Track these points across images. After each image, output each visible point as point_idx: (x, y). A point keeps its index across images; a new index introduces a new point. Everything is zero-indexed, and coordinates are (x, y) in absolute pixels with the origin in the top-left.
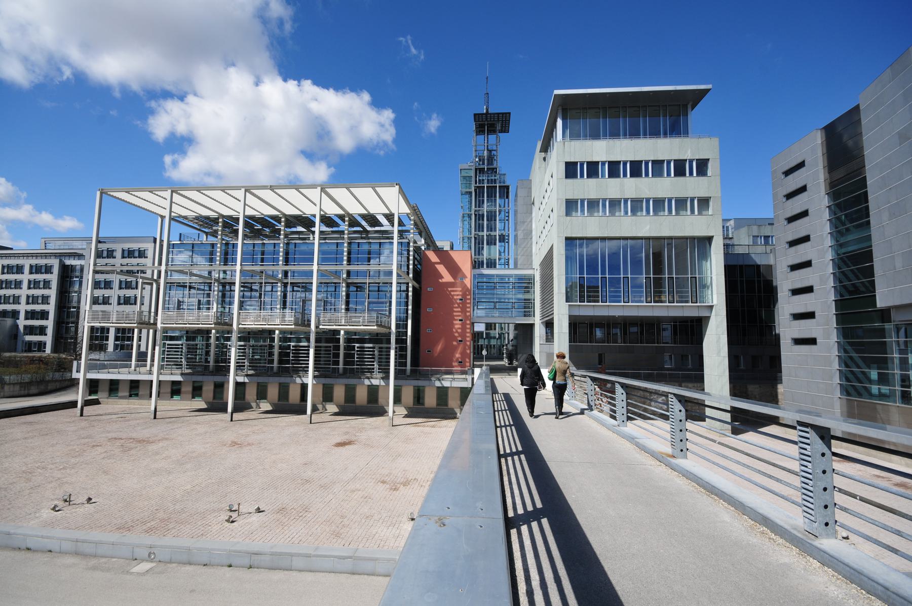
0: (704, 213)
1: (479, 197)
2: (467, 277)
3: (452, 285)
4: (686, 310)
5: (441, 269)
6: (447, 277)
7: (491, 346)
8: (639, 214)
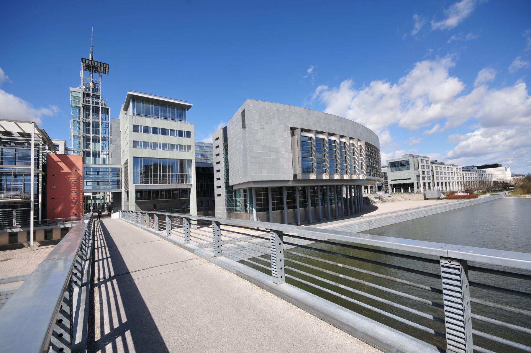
0: (189, 151)
1: (86, 111)
2: (79, 170)
3: (68, 174)
4: (184, 186)
5: (62, 165)
6: (66, 169)
7: (96, 204)
8: (165, 149)
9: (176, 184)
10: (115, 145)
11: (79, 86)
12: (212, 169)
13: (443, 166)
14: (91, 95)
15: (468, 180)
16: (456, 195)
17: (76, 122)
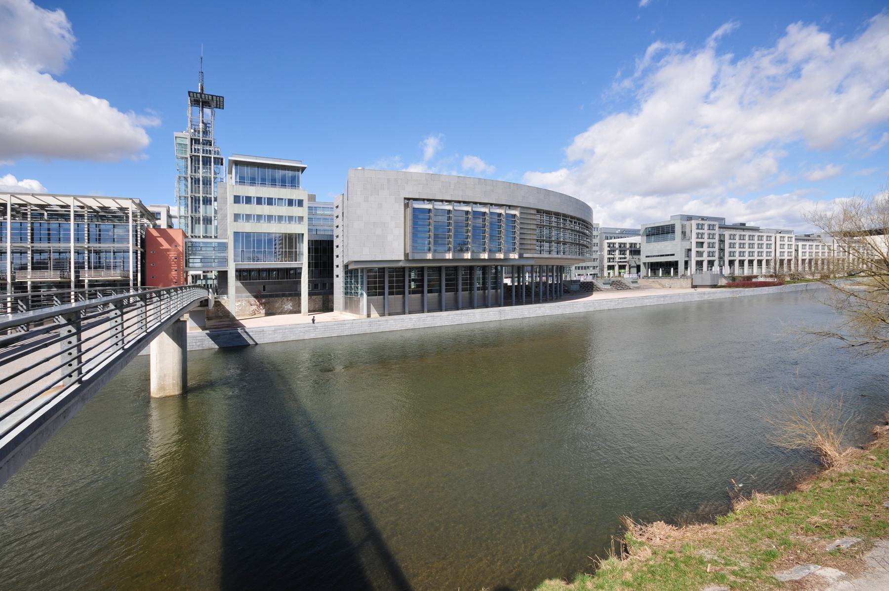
3: (168, 250)
5: (161, 240)
7: (208, 285)
9: (273, 262)
10: (221, 214)
11: (185, 130)
12: (332, 242)
13: (757, 234)
14: (201, 141)
15: (814, 256)
16: (753, 281)
17: (183, 179)
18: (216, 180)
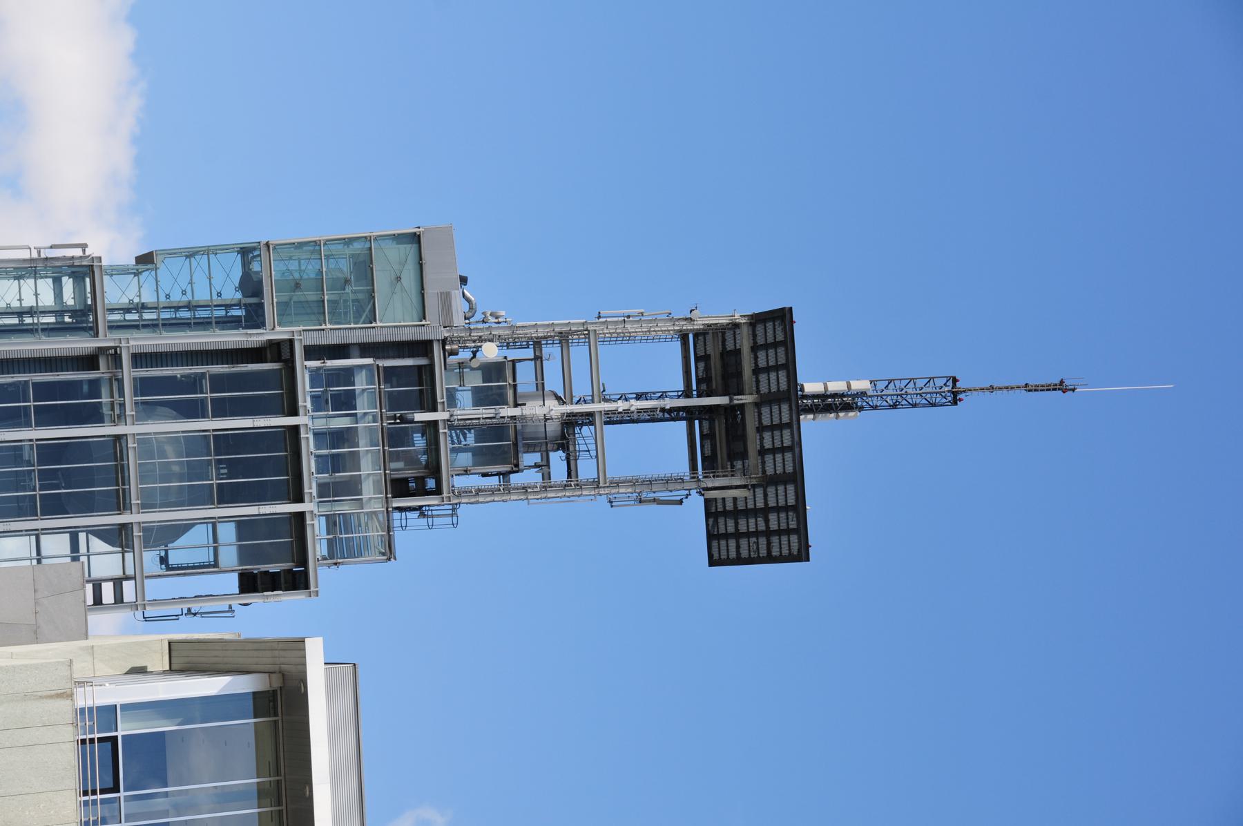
18: (98, 544)
